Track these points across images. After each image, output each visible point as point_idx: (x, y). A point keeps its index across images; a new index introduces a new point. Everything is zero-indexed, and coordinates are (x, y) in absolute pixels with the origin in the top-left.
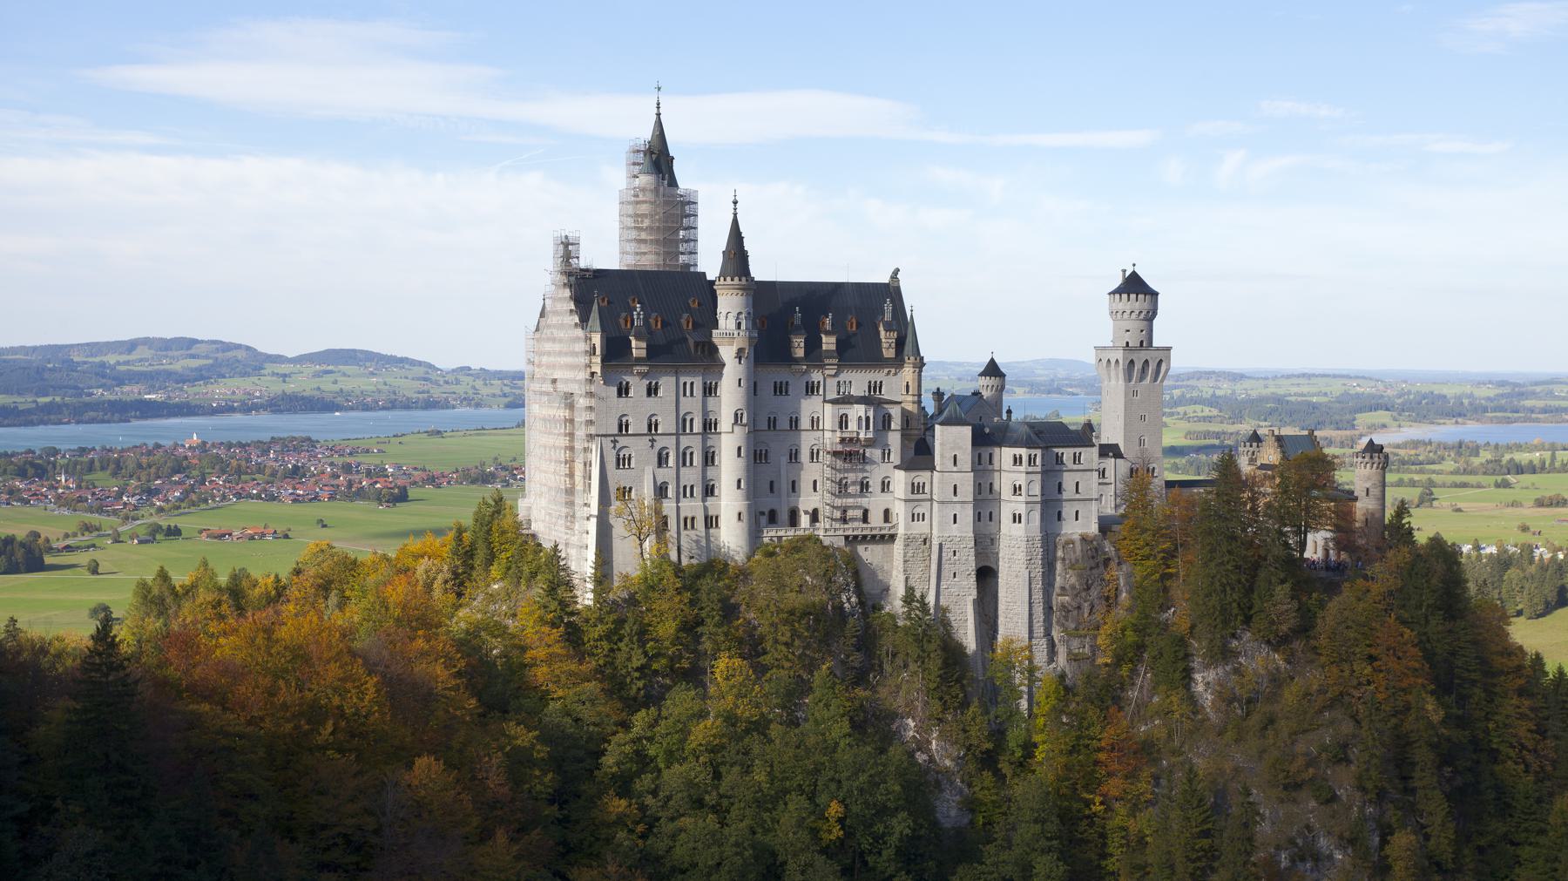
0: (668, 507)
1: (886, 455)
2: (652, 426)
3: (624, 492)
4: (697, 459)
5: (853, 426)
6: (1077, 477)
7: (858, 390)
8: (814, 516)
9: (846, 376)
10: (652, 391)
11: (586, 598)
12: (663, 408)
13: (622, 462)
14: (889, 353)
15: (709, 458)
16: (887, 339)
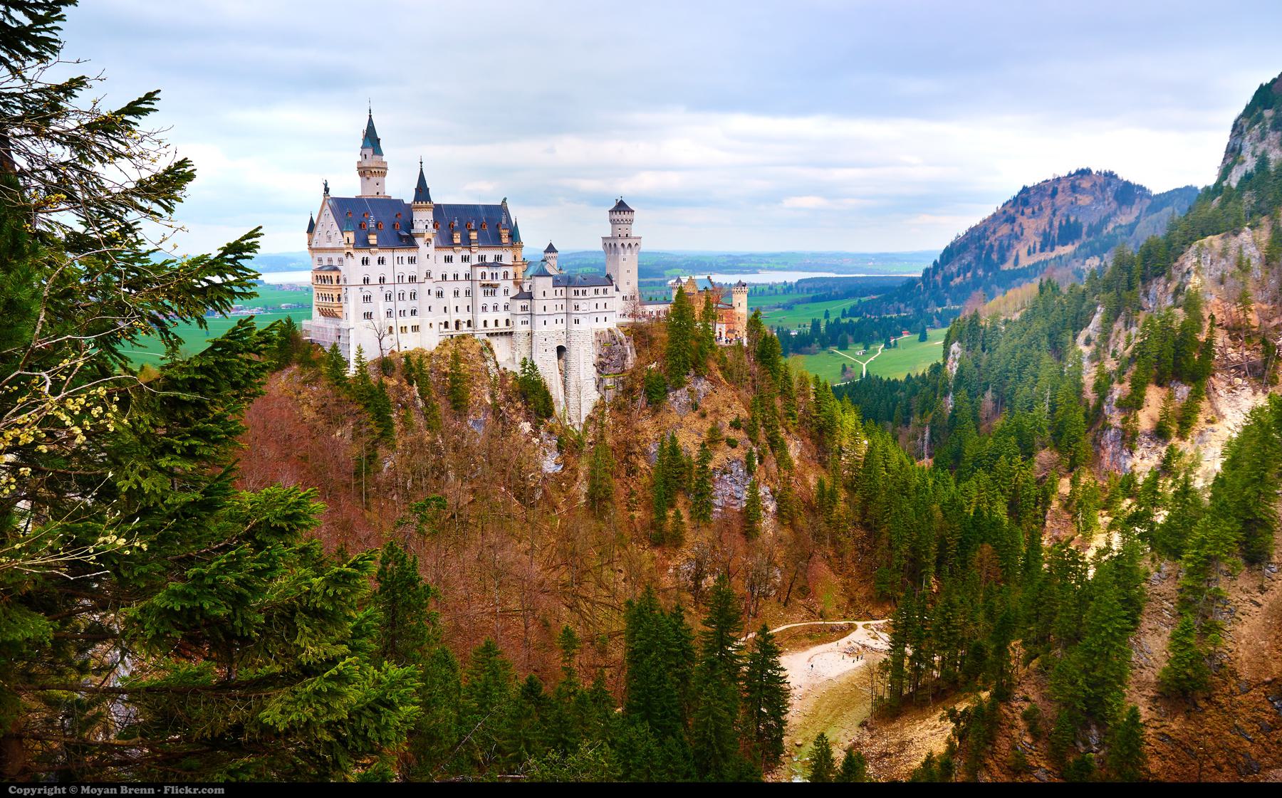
0: (392, 322)
1: (506, 292)
2: (382, 280)
3: (368, 316)
4: (407, 296)
5: (488, 277)
6: (605, 301)
7: (490, 259)
8: (469, 323)
9: (482, 252)
10: (381, 261)
11: (352, 371)
12: (387, 270)
13: (367, 299)
14: (505, 240)
15: (413, 296)
16: (505, 234)
